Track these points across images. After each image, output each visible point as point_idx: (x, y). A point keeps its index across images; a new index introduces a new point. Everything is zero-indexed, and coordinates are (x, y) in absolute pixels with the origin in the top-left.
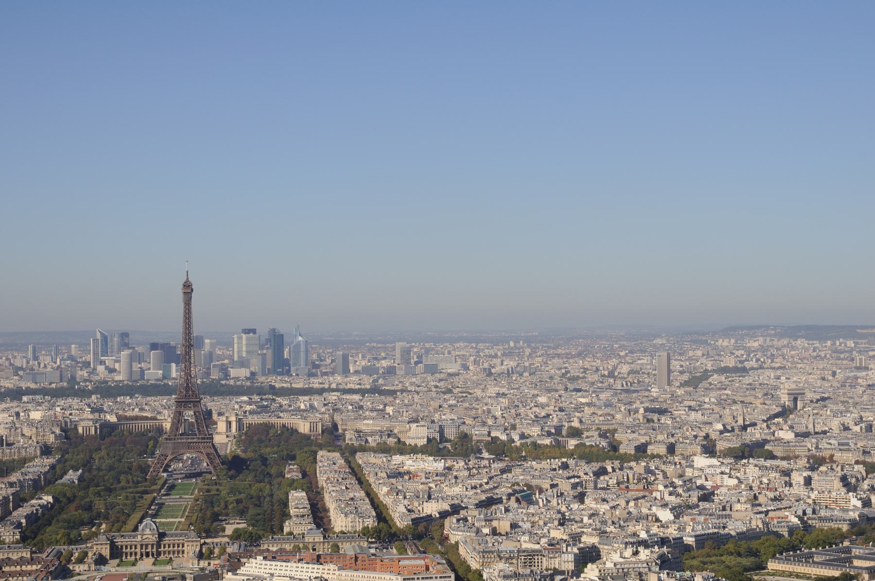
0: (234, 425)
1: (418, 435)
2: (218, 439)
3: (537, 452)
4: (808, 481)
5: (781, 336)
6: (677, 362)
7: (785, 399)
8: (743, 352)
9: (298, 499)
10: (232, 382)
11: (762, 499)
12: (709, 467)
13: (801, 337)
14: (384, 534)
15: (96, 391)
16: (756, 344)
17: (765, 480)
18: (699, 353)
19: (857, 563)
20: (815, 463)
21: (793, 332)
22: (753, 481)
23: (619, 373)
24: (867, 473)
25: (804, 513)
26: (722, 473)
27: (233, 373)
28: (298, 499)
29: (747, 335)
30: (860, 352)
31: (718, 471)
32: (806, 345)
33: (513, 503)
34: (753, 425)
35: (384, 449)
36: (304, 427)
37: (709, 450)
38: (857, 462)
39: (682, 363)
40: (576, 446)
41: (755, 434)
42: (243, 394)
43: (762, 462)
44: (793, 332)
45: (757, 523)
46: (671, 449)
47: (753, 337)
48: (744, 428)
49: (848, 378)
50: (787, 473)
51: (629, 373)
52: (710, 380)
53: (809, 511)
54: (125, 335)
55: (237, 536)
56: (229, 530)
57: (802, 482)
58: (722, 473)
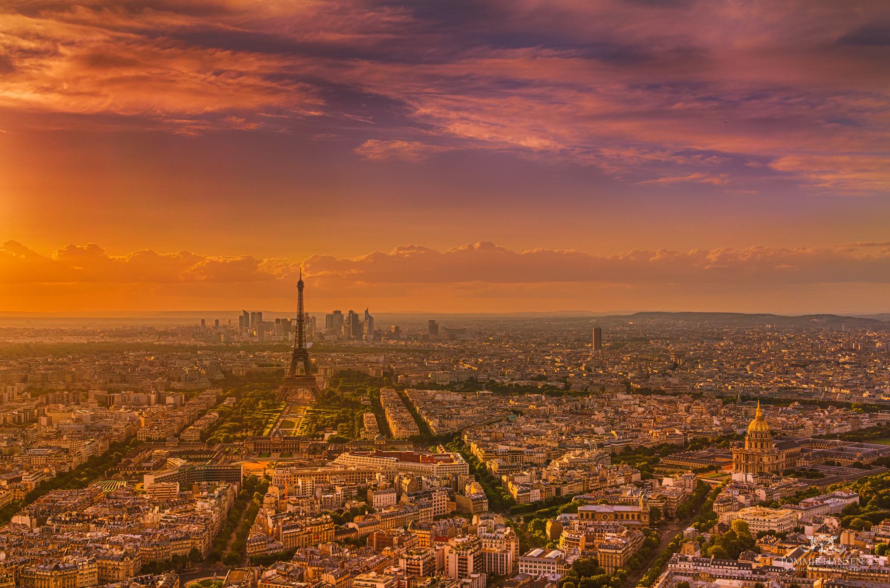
0: (328, 371)
1: (444, 377)
2: (317, 379)
3: (521, 391)
4: (688, 410)
7: (673, 359)
9: (369, 417)
10: (326, 344)
14: (425, 439)
15: (243, 348)
19: (718, 460)
24: (725, 403)
25: (685, 429)
27: (327, 338)
28: (369, 417)
33: (504, 422)
35: (421, 386)
36: (372, 373)
38: (717, 397)
40: (544, 386)
42: (333, 351)
43: (659, 397)
54: (260, 314)
55: (333, 440)
56: (327, 436)
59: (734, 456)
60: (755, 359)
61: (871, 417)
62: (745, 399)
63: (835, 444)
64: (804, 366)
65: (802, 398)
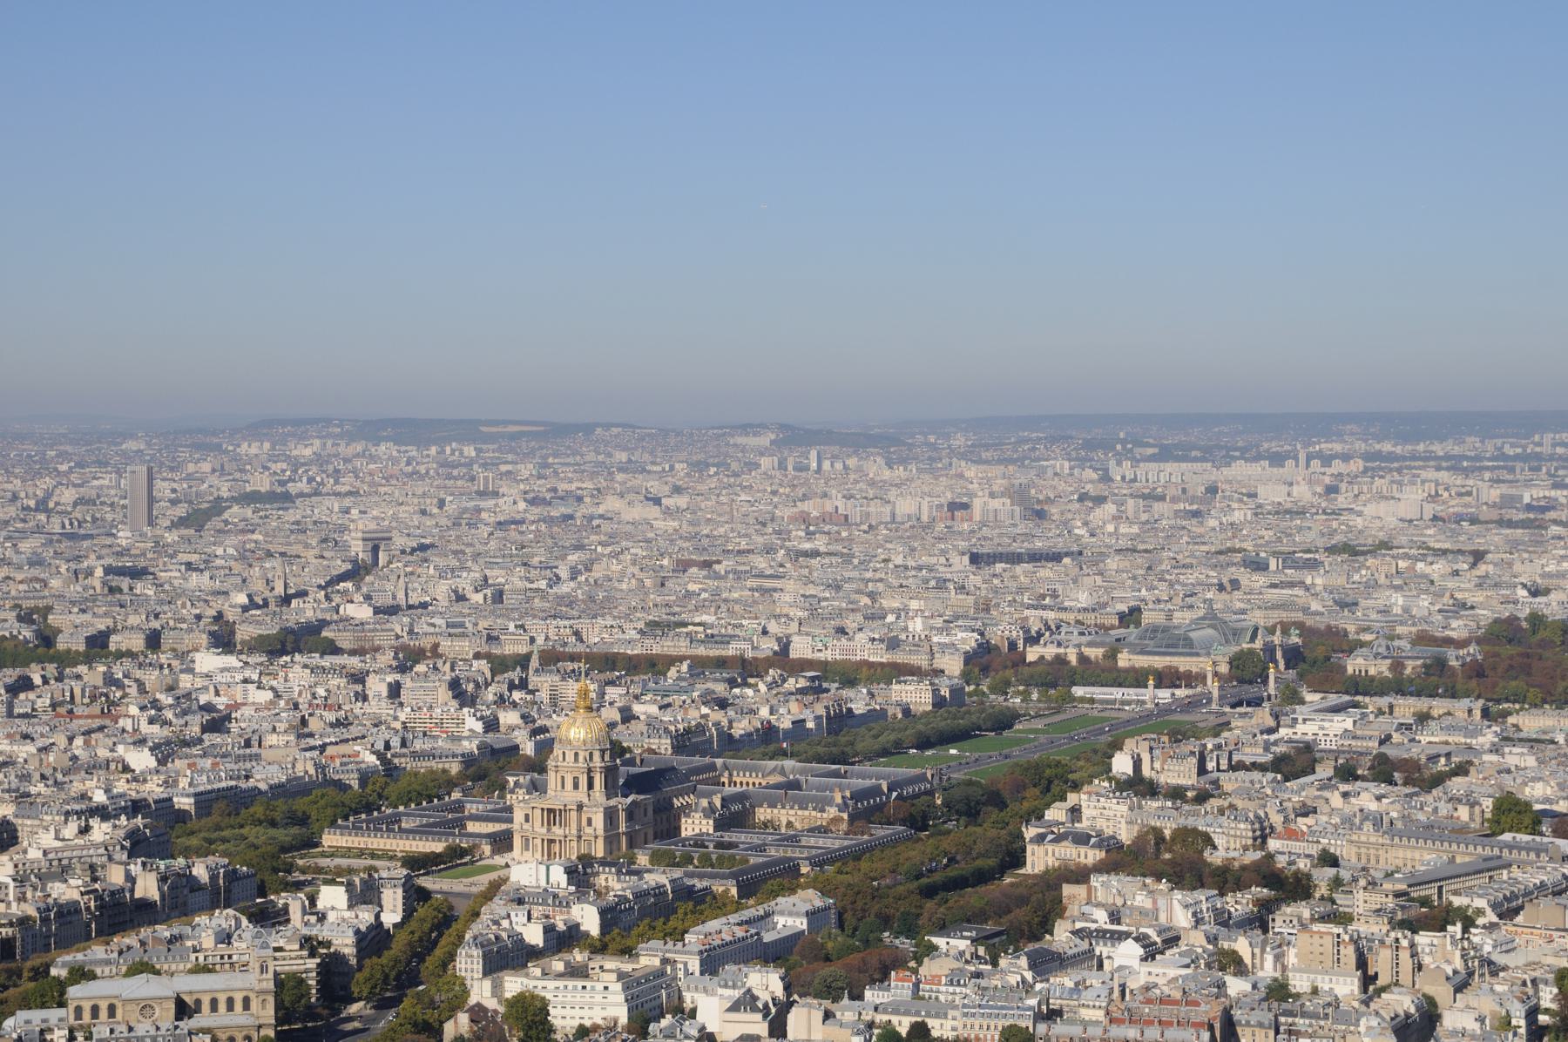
4: (395, 691)
5: (351, 438)
6: (165, 484)
7: (358, 549)
8: (284, 466)
11: (314, 725)
12: (223, 670)
13: (387, 439)
16: (308, 452)
17: (321, 692)
18: (206, 467)
19: (472, 827)
20: (408, 659)
21: (371, 430)
22: (300, 694)
23: (57, 504)
24: (494, 673)
25: (387, 746)
26: (245, 681)
29: (293, 435)
30: (484, 466)
31: (239, 677)
32: (395, 453)
34: (302, 594)
37: (223, 640)
38: (477, 656)
39: (175, 485)
41: (305, 611)
43: (316, 659)
44: (371, 430)
45: (305, 767)
46: (154, 641)
47: (302, 438)
48: (286, 600)
49: (465, 510)
50: (359, 678)
51: (75, 504)
52: (226, 516)
53: (395, 742)
57: (385, 693)
58: (245, 681)
59: (518, 816)
60: (579, 547)
61: (872, 695)
62: (551, 659)
63: (782, 772)
64: (707, 565)
65: (701, 651)
